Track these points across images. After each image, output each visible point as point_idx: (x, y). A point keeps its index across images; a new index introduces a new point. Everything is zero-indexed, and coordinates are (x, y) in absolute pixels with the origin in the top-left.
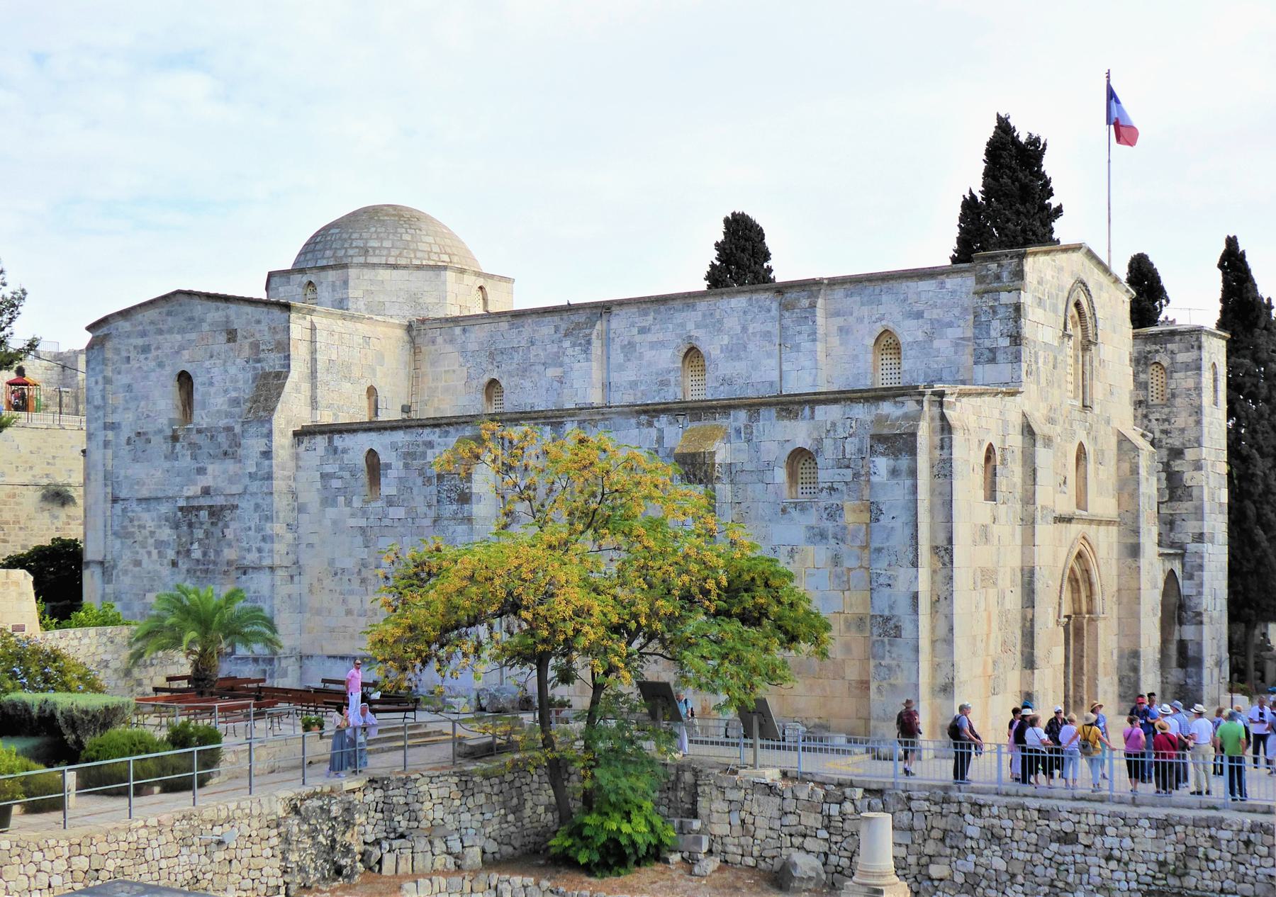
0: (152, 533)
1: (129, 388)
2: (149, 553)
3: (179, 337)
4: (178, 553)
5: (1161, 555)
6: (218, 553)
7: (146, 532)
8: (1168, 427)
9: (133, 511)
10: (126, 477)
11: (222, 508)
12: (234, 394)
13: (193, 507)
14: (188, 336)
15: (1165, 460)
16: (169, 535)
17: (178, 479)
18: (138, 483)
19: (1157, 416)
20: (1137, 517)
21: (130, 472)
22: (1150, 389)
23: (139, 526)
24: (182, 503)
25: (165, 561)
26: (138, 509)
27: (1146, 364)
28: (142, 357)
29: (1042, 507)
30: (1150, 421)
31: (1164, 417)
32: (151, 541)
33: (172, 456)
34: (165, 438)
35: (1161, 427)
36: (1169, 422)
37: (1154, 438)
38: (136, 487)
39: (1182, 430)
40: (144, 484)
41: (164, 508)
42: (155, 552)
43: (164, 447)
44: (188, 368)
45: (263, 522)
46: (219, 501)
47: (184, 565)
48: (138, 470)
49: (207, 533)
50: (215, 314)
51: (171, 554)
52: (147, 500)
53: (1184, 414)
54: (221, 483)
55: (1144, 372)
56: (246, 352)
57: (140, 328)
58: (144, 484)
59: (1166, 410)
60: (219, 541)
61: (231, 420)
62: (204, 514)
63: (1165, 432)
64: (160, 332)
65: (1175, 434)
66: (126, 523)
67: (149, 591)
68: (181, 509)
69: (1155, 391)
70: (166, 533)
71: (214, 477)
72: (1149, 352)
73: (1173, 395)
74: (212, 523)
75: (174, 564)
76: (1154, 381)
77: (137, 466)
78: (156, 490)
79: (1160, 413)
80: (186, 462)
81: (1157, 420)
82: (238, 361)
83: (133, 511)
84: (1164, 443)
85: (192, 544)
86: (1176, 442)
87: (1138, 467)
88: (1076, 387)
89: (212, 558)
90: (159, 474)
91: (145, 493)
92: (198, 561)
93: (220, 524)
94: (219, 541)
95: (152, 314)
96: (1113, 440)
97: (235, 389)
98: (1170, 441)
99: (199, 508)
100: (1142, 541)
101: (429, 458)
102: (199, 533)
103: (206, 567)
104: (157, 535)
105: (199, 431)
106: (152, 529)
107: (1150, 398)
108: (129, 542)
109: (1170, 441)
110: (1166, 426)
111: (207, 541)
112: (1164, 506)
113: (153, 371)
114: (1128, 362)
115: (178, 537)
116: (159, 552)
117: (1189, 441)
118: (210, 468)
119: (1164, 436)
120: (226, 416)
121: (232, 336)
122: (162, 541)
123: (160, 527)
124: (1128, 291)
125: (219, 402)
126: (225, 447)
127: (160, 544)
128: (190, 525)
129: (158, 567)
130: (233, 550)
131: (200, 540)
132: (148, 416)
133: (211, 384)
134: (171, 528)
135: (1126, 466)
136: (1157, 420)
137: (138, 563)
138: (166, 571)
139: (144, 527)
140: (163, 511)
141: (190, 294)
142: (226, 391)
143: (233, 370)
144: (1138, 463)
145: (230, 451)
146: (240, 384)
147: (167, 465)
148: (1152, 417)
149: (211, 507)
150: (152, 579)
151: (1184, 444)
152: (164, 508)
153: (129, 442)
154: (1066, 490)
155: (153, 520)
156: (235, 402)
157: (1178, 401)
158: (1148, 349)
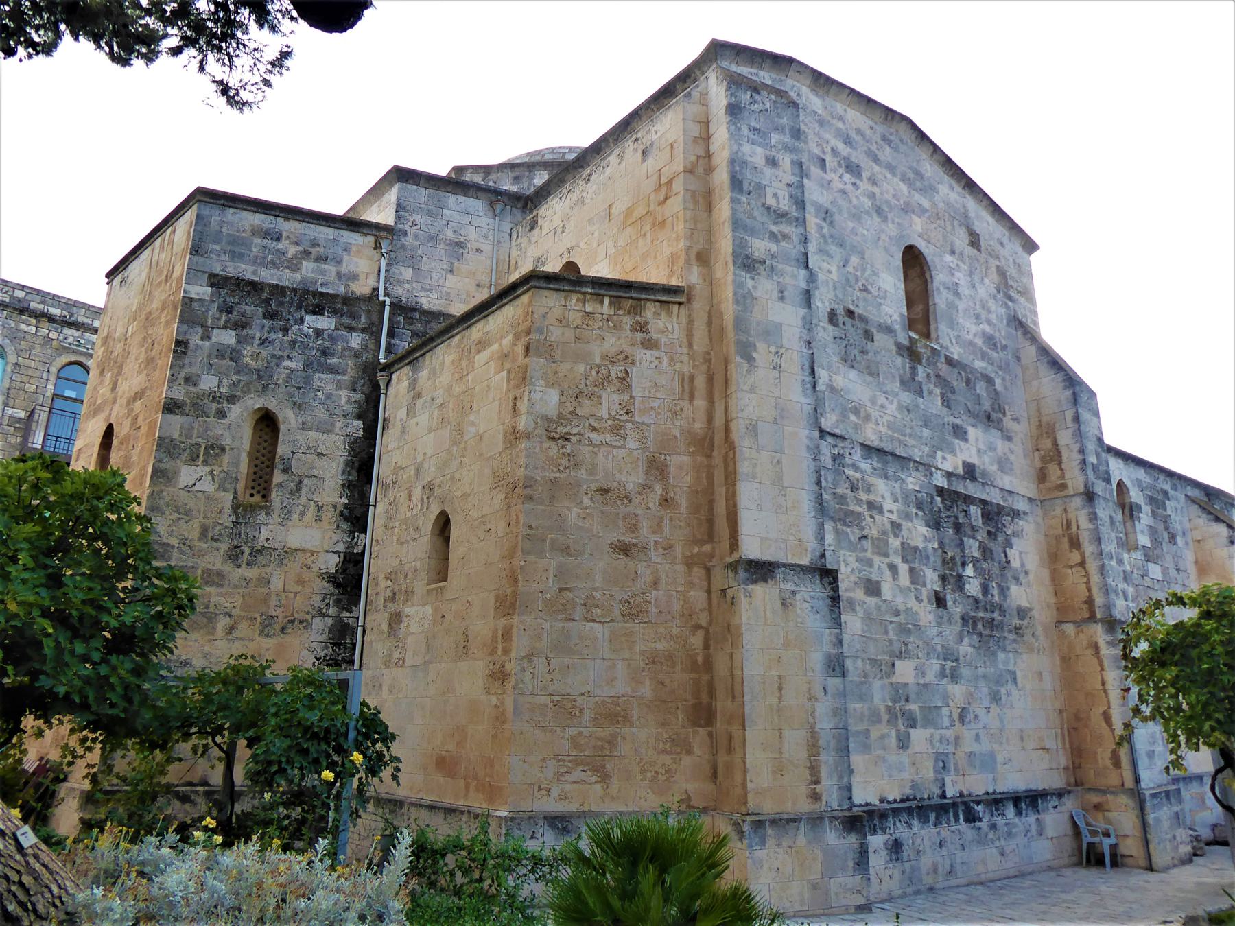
0: (896, 526)
1: (826, 214)
2: (893, 568)
3: (904, 188)
4: (943, 578)
6: (1003, 591)
7: (884, 520)
9: (855, 467)
10: (832, 389)
11: (1000, 510)
12: (988, 329)
13: (959, 494)
14: (917, 197)
16: (926, 539)
17: (926, 433)
18: (856, 411)
21: (839, 381)
23: (871, 505)
24: (941, 481)
25: (924, 593)
26: (865, 465)
28: (847, 177)
32: (895, 543)
33: (910, 383)
34: (899, 346)
38: (853, 418)
40: (867, 418)
41: (913, 481)
42: (903, 568)
43: (899, 360)
44: (921, 245)
45: (1120, 550)
46: (994, 497)
47: (956, 608)
48: (851, 383)
49: (984, 549)
50: (949, 192)
51: (931, 578)
52: (880, 452)
54: (985, 463)
56: (994, 276)
57: (840, 125)
58: (867, 418)
60: (1002, 569)
61: (990, 368)
62: (975, 511)
64: (876, 160)
66: (843, 489)
67: (901, 656)
68: (940, 491)
70: (919, 533)
71: (979, 451)
74: (989, 533)
75: (940, 601)
77: (853, 374)
78: (892, 439)
80: (933, 404)
82: (986, 281)
83: (855, 467)
85: (964, 564)
89: (996, 598)
90: (892, 408)
91: (871, 435)
92: (976, 601)
93: (1001, 539)
94: (1002, 569)
95: (855, 118)
97: (989, 322)
99: (968, 500)
101: (1169, 512)
102: (972, 547)
103: (988, 615)
104: (904, 533)
105: (950, 362)
106: (895, 517)
108: (853, 533)
111: (985, 565)
113: (868, 213)
115: (941, 543)
116: (912, 570)
118: (972, 433)
120: (983, 359)
121: (975, 240)
122: (916, 549)
123: (908, 517)
125: (971, 329)
126: (987, 405)
127: (909, 553)
128: (958, 527)
129: (912, 603)
130: (1022, 588)
131: (975, 561)
132: (866, 290)
133: (957, 294)
134: (928, 526)
137: (873, 589)
138: (926, 613)
139: (880, 510)
140: (911, 487)
141: (922, 137)
142: (977, 317)
143: (982, 292)
145: (994, 415)
146: (993, 317)
147: (906, 398)
149: (984, 503)
150: (903, 630)
152: (913, 481)
153: (832, 317)
155: (896, 500)
156: (990, 340)
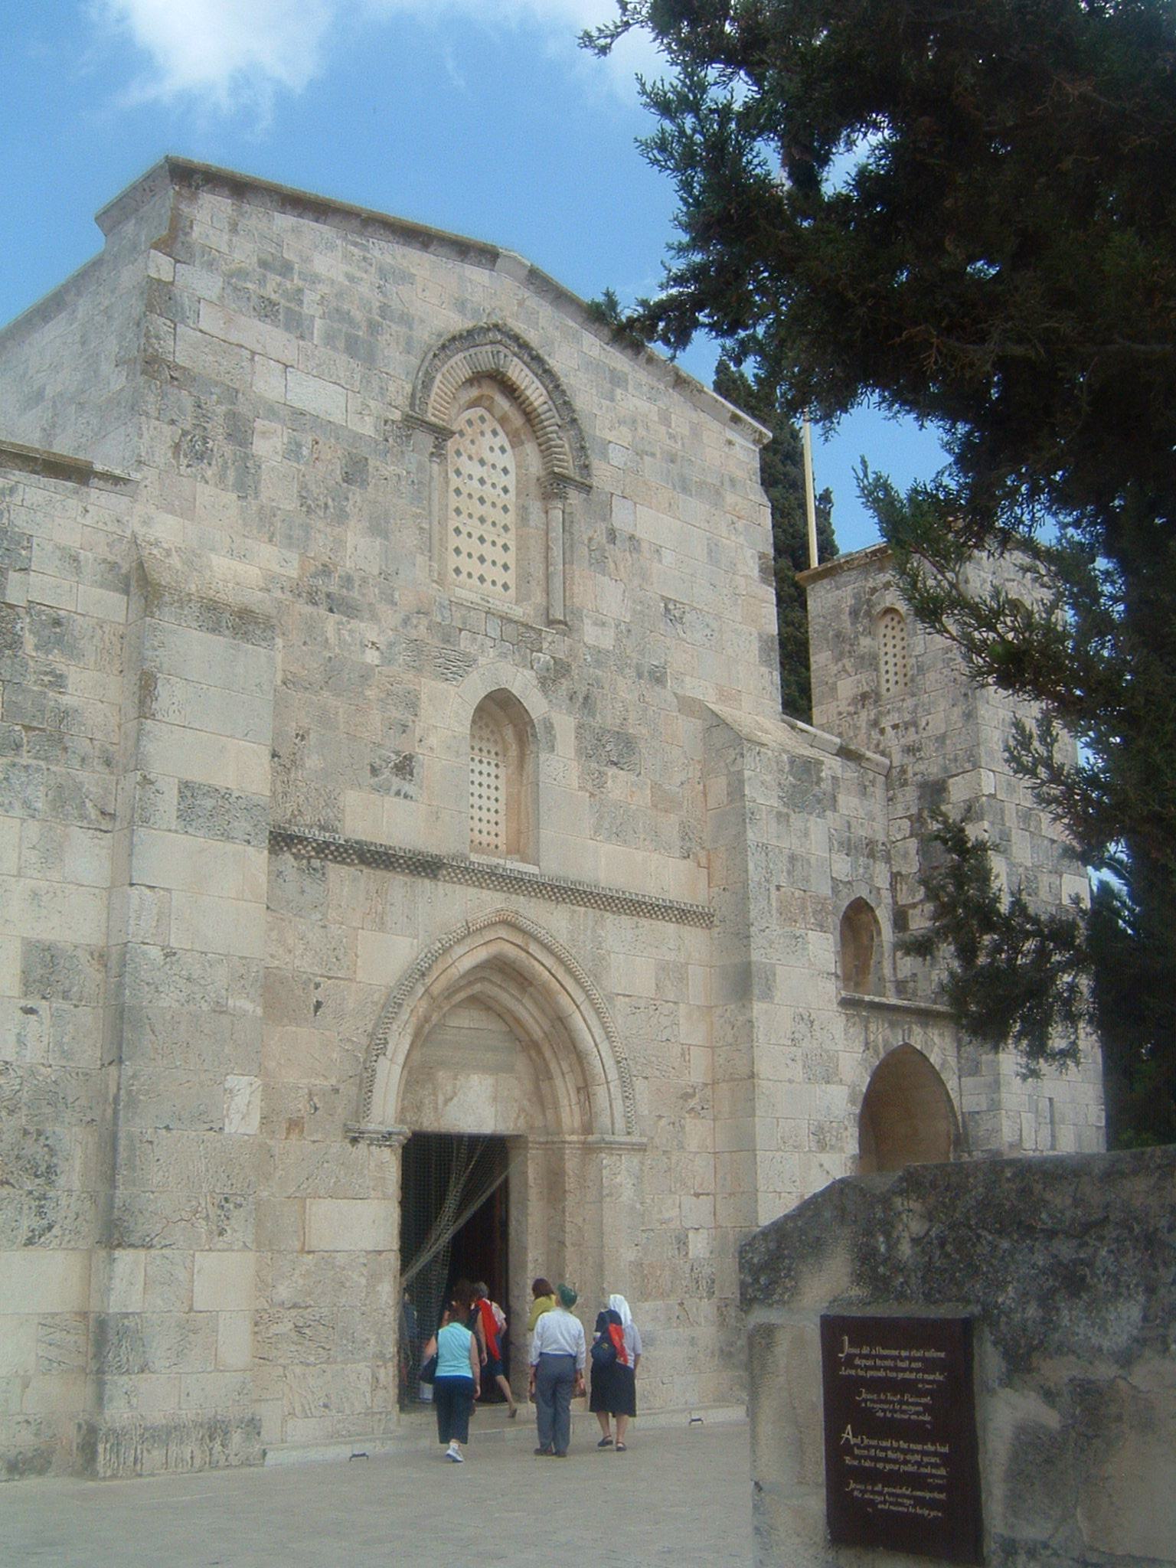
5: (845, 1003)
8: (915, 737)
15: (914, 811)
19: (894, 718)
20: (746, 898)
22: (883, 668)
27: (868, 614)
29: (187, 789)
30: (882, 731)
31: (907, 717)
35: (903, 741)
36: (915, 724)
37: (891, 767)
39: (941, 739)
53: (943, 704)
55: (870, 633)
59: (910, 702)
63: (910, 750)
65: (929, 750)
69: (892, 670)
72: (874, 590)
73: (921, 669)
76: (889, 649)
79: (899, 710)
81: (895, 727)
84: (910, 774)
86: (932, 769)
87: (741, 782)
88: (524, 578)
96: (687, 728)
98: (920, 767)
100: (756, 956)
107: (884, 686)
109: (920, 767)
110: (911, 737)
112: (917, 911)
114: (755, 573)
117: (956, 760)
119: (912, 759)
124: (735, 419)
135: (719, 785)
136: (895, 727)
144: (740, 772)
148: (886, 723)
151: (945, 769)
154: (407, 788)
157: (932, 676)
158: (871, 584)
